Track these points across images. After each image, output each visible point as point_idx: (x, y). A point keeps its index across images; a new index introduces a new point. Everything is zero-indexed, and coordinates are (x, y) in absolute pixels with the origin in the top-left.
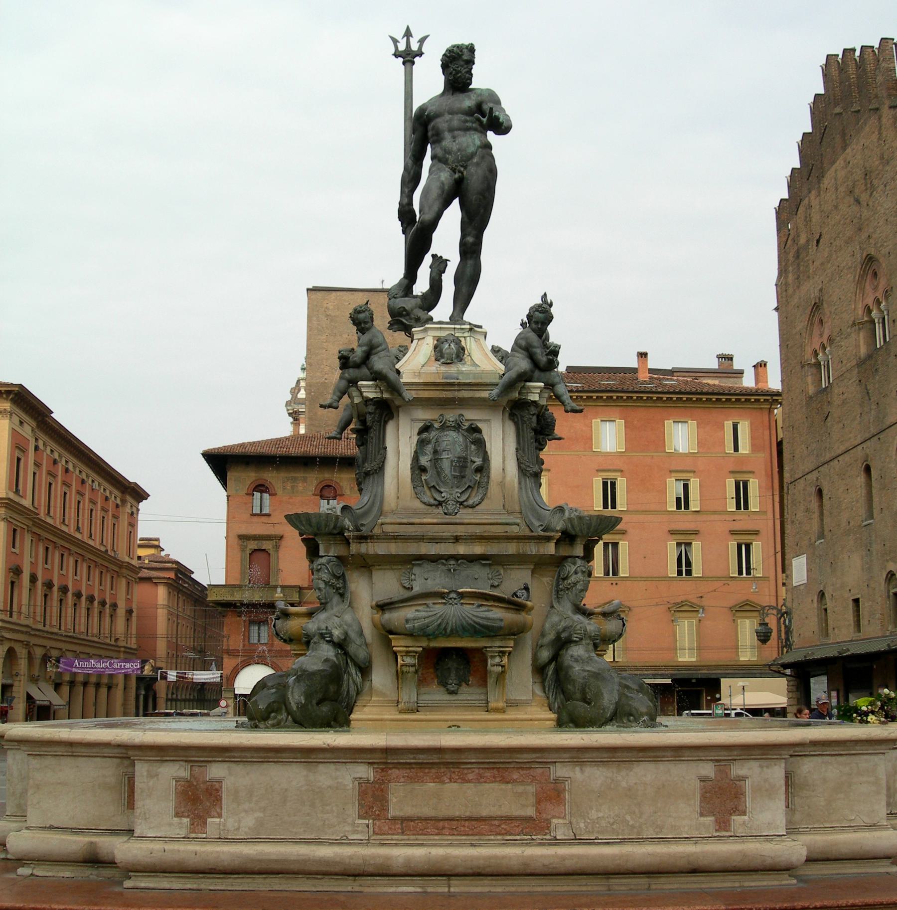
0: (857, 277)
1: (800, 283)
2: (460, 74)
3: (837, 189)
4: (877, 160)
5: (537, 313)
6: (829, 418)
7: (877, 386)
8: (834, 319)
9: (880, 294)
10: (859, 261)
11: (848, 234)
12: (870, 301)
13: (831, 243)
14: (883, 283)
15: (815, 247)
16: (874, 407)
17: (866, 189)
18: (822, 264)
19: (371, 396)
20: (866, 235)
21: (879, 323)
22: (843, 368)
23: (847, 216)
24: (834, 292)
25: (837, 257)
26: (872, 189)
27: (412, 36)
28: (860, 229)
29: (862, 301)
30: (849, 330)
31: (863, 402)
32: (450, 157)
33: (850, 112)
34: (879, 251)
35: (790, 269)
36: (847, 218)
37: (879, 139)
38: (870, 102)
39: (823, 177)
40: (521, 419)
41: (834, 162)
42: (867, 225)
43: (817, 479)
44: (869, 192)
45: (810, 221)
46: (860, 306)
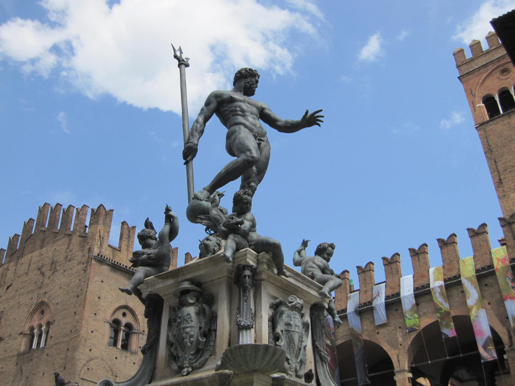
0: (31, 310)
2: (253, 86)
3: (29, 265)
4: (63, 258)
5: (330, 248)
7: (29, 368)
8: (7, 328)
9: (43, 322)
10: (35, 303)
11: (31, 288)
12: (35, 324)
13: (17, 290)
14: (47, 317)
15: (5, 289)
16: (24, 378)
17: (50, 270)
18: (7, 299)
19: (252, 263)
20: (44, 291)
21: (37, 336)
22: (6, 355)
23: (33, 279)
25: (20, 298)
26: (55, 270)
27: (182, 53)
28: (40, 288)
29: (30, 323)
30: (17, 336)
31: (16, 375)
32: (255, 128)
33: (51, 232)
34: (51, 301)
36: (33, 281)
37: (67, 248)
38: (66, 231)
39: (22, 257)
40: (318, 318)
41: (32, 252)
42: (47, 286)
44: (52, 271)
45: (6, 276)
46: (28, 325)
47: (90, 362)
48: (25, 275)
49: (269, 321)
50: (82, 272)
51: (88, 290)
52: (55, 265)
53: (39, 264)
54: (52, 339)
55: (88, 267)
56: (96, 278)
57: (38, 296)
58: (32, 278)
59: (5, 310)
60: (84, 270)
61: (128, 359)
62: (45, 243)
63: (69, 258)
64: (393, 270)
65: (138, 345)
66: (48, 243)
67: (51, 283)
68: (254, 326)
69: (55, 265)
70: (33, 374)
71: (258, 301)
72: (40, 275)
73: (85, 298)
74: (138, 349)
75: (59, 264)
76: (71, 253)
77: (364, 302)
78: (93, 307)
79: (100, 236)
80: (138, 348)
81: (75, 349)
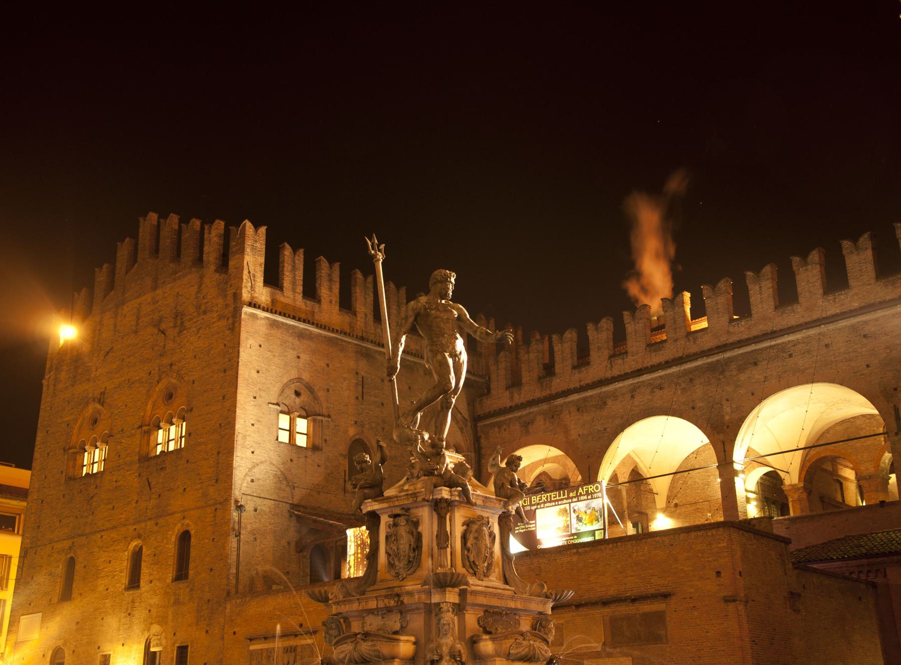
1: (75, 382)
3: (138, 318)
6: (95, 499)
7: (161, 480)
17: (175, 327)
22: (121, 461)
23: (148, 342)
24: (120, 398)
26: (182, 329)
28: (161, 355)
30: (133, 431)
31: (141, 491)
34: (182, 378)
35: (65, 368)
37: (198, 292)
39: (123, 304)
41: (139, 297)
43: (70, 548)
44: (177, 329)
47: (254, 470)
48: (133, 335)
49: (461, 537)
50: (227, 332)
51: (240, 360)
52: (181, 319)
53: (154, 316)
54: (192, 436)
55: (237, 325)
56: (251, 341)
57: (159, 369)
58: (146, 339)
59: (107, 392)
60: (230, 329)
61: (309, 460)
62: (158, 282)
63: (203, 308)
64: (719, 306)
65: (322, 438)
66: (164, 282)
67: (179, 349)
68: (449, 546)
69: (181, 319)
70: (169, 490)
71: (452, 523)
72: (158, 334)
73: (237, 373)
74: (322, 444)
75: (188, 317)
76: (205, 301)
77: (672, 357)
78: (249, 385)
79: (249, 272)
80: (322, 441)
81: (230, 451)
